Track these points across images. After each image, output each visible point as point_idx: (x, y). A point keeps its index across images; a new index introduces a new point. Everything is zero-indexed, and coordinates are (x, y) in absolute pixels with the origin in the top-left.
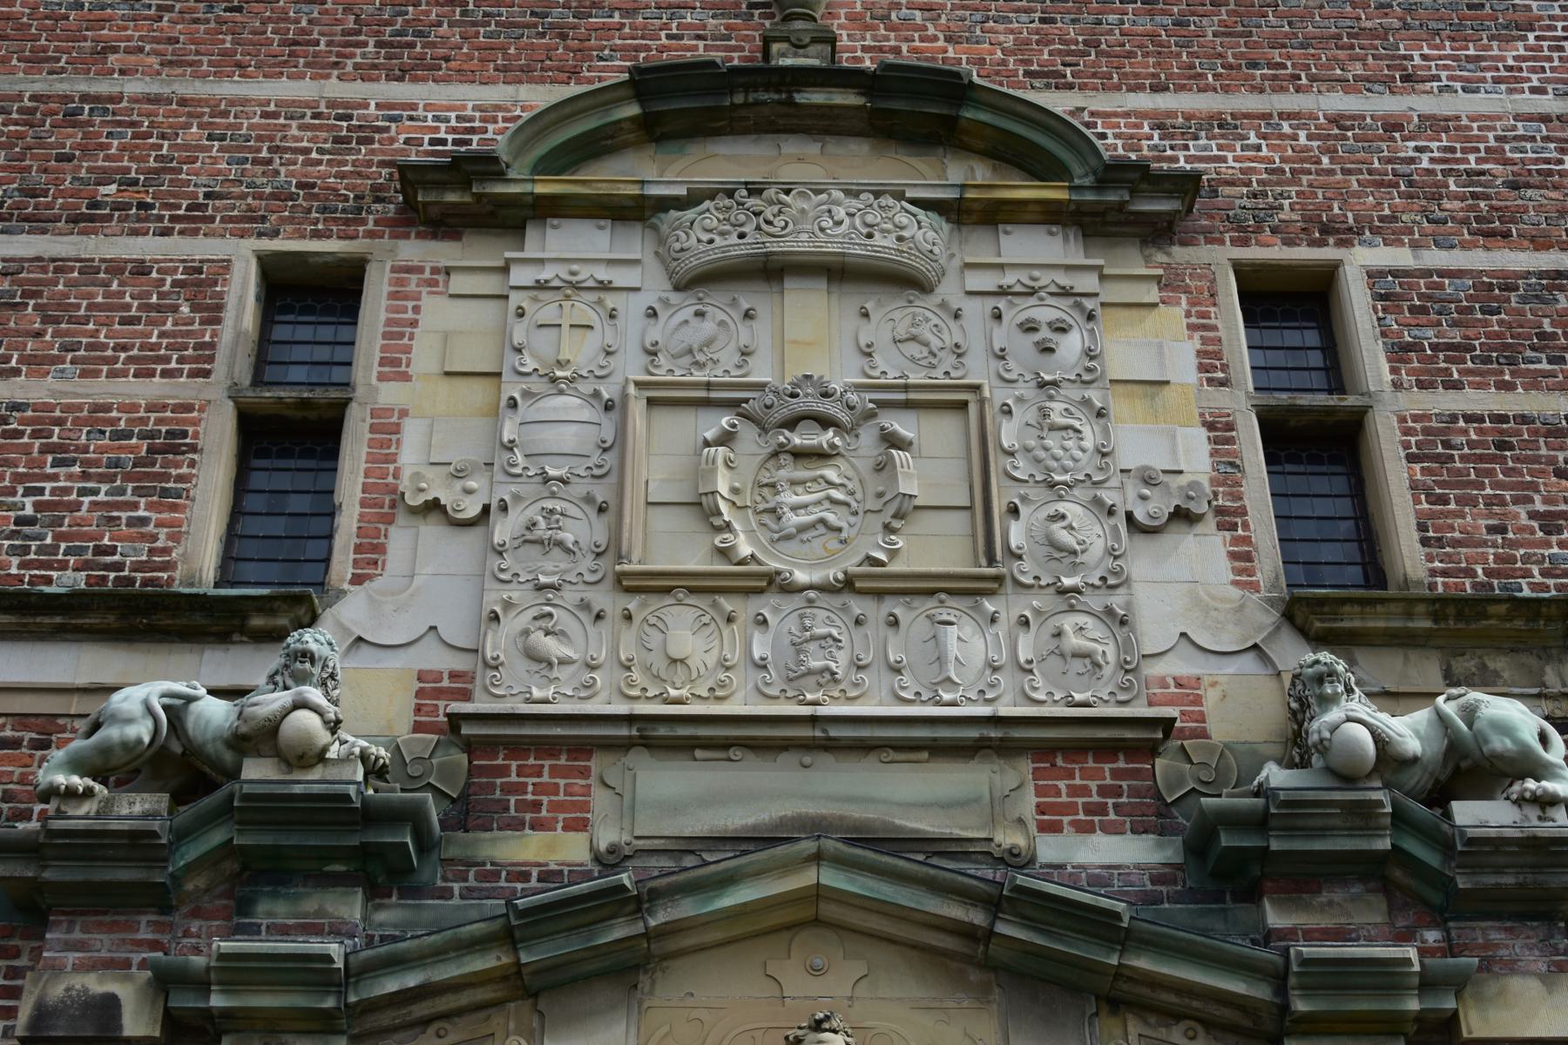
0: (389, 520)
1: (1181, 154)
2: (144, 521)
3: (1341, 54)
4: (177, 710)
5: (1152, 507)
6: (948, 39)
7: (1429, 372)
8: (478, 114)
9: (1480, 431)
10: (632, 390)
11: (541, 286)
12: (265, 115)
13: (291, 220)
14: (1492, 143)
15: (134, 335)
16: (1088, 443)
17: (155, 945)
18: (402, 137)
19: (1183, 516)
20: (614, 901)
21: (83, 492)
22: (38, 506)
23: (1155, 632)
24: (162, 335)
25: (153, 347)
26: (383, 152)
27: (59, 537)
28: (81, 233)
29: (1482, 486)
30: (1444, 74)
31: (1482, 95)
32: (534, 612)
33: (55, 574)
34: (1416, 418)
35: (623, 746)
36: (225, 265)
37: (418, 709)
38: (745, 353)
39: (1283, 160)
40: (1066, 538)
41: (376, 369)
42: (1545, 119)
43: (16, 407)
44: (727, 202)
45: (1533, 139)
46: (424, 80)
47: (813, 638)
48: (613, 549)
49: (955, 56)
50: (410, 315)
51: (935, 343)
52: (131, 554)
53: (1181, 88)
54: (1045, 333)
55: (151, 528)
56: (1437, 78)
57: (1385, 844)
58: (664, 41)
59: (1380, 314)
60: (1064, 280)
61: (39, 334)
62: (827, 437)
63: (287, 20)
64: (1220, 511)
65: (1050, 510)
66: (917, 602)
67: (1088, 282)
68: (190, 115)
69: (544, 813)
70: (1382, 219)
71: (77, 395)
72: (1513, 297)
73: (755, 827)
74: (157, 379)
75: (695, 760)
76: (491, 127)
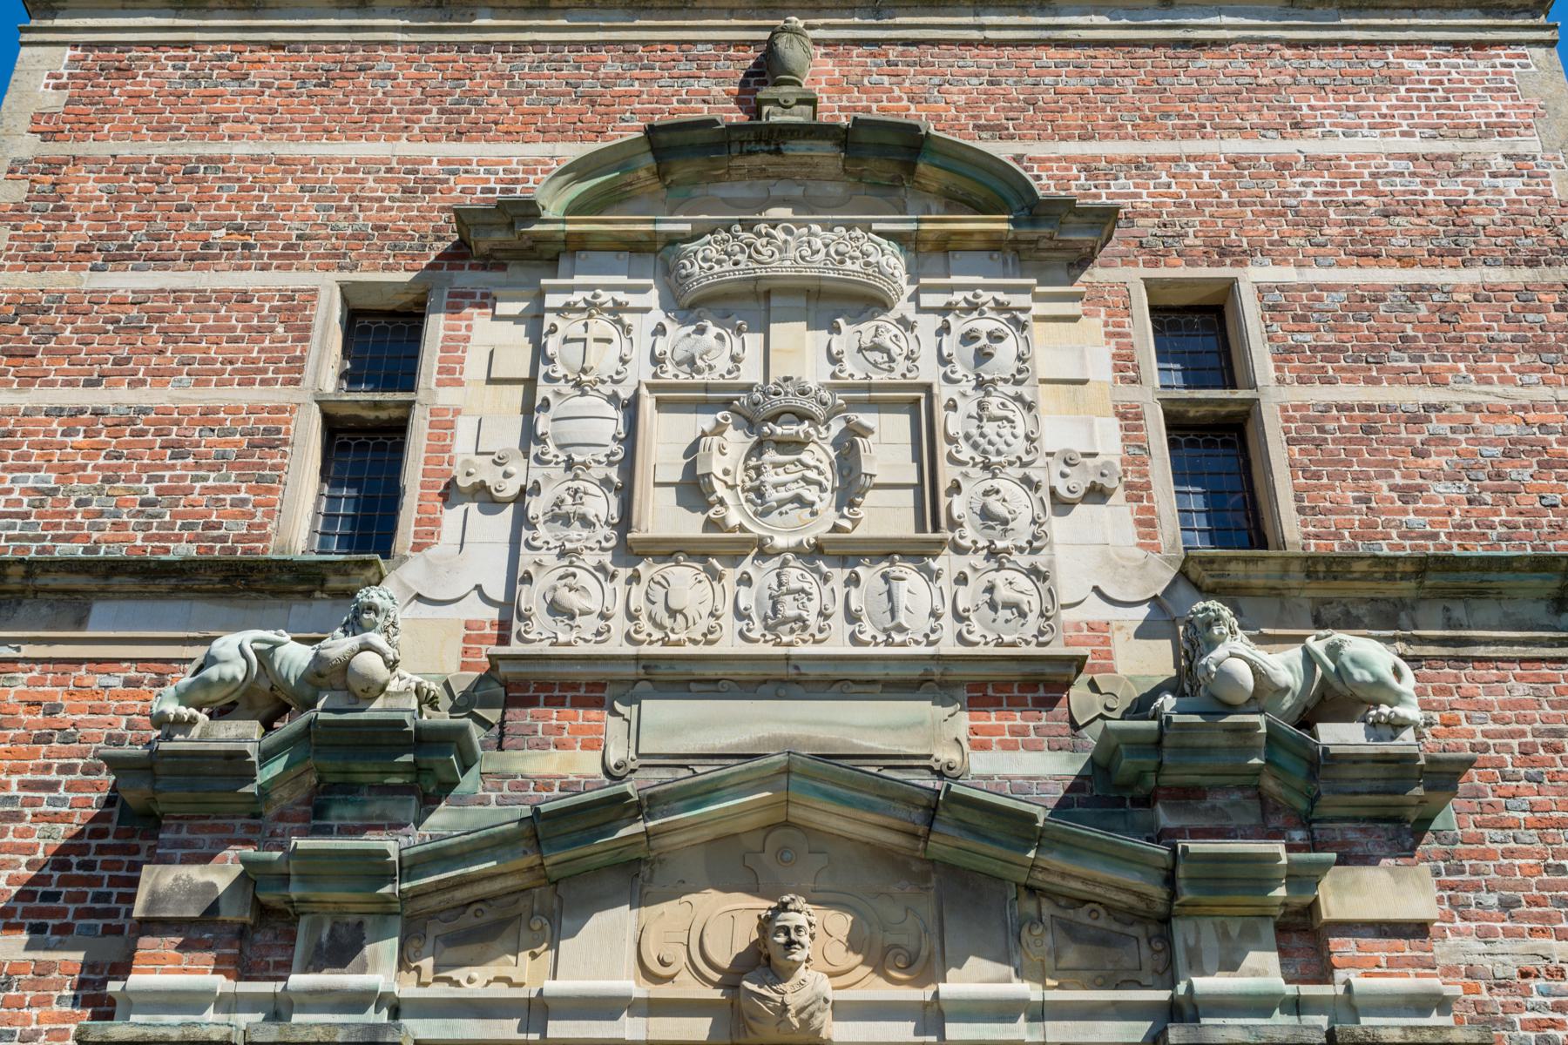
1: (1103, 192)
2: (244, 502)
3: (1241, 107)
5: (1071, 482)
6: (911, 100)
8: (521, 167)
9: (1351, 419)
10: (644, 391)
11: (568, 308)
12: (347, 171)
13: (367, 257)
14: (1367, 179)
15: (238, 351)
16: (1020, 431)
18: (459, 188)
19: (1097, 494)
20: (616, 808)
21: (195, 479)
22: (159, 491)
26: (444, 200)
27: (174, 516)
28: (196, 269)
29: (1350, 464)
30: (1327, 122)
31: (1359, 138)
32: (561, 571)
33: (172, 546)
34: (1296, 408)
36: (313, 293)
37: (465, 652)
38: (735, 359)
41: (435, 376)
42: (1413, 158)
43: (143, 411)
44: (725, 235)
45: (1402, 175)
46: (478, 140)
47: (789, 592)
48: (625, 522)
49: (915, 114)
50: (463, 332)
51: (895, 350)
52: (235, 528)
53: (1106, 136)
56: (1319, 125)
58: (676, 105)
59: (1268, 322)
61: (161, 352)
64: (1128, 486)
65: (987, 485)
68: (285, 172)
69: (565, 735)
70: (1272, 243)
71: (191, 400)
72: (1382, 307)
73: (737, 746)
74: (257, 387)
75: (690, 691)
76: (532, 178)
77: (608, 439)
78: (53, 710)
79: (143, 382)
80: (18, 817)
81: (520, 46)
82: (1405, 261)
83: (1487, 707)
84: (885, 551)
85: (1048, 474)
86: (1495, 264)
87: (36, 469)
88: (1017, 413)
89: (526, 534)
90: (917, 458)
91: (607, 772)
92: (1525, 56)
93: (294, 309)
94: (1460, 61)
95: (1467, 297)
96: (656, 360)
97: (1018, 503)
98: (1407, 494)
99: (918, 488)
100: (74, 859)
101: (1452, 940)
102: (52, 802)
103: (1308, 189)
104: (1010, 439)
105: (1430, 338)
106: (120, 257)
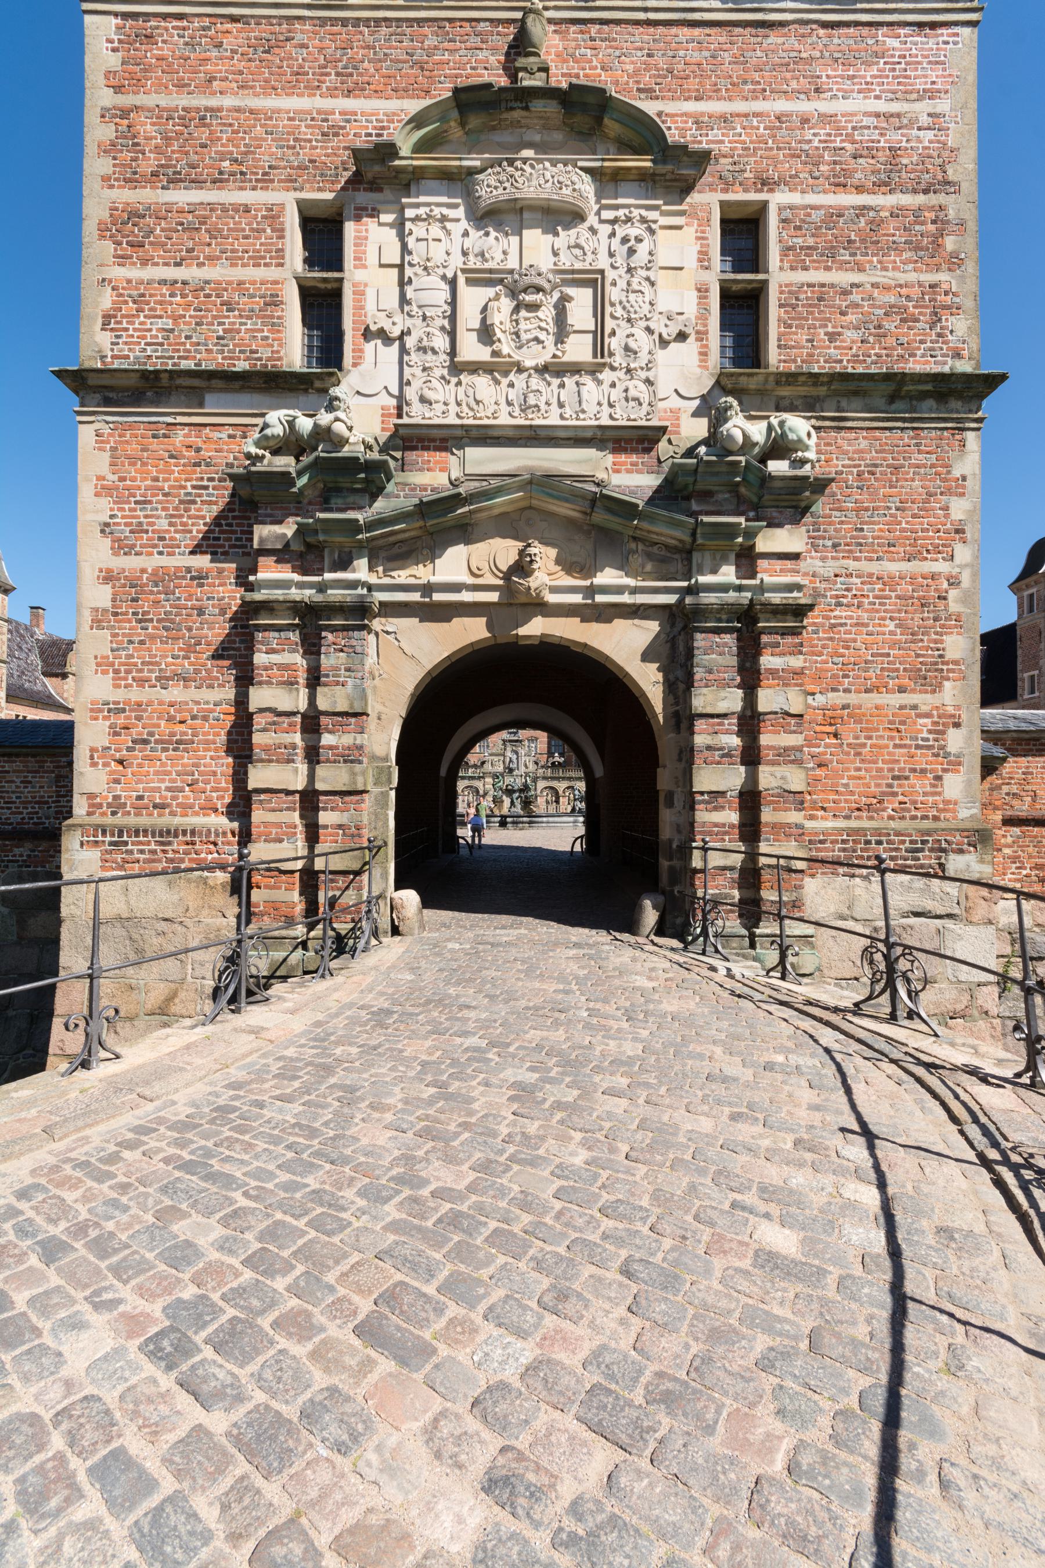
1: (704, 139)
2: (267, 338)
3: (788, 75)
5: (669, 330)
6: (602, 68)
9: (813, 292)
10: (459, 273)
11: (417, 219)
12: (290, 119)
13: (308, 181)
15: (249, 244)
16: (647, 300)
19: (682, 337)
20: (456, 500)
21: (241, 324)
22: (225, 331)
23: (664, 388)
24: (261, 244)
27: (235, 345)
28: (219, 189)
29: (807, 319)
30: (835, 87)
34: (787, 285)
38: (505, 253)
39: (751, 142)
40: (633, 345)
42: (877, 115)
43: (207, 282)
44: (498, 169)
48: (453, 352)
49: (603, 80)
51: (587, 248)
52: (265, 353)
53: (710, 98)
56: (831, 90)
61: (209, 245)
63: (291, 58)
64: (698, 332)
65: (628, 332)
72: (841, 220)
77: (442, 303)
78: (198, 450)
79: (203, 264)
80: (194, 502)
82: (859, 189)
83: (846, 453)
84: (575, 369)
85: (658, 325)
87: (161, 317)
88: (646, 287)
89: (406, 358)
90: (595, 315)
91: (451, 483)
92: (957, 35)
93: (273, 214)
94: (919, 39)
95: (887, 214)
96: (465, 254)
97: (643, 342)
98: (832, 337)
99: (595, 333)
101: (809, 560)
102: (208, 495)
103: (815, 137)
105: (863, 241)
106: (175, 181)
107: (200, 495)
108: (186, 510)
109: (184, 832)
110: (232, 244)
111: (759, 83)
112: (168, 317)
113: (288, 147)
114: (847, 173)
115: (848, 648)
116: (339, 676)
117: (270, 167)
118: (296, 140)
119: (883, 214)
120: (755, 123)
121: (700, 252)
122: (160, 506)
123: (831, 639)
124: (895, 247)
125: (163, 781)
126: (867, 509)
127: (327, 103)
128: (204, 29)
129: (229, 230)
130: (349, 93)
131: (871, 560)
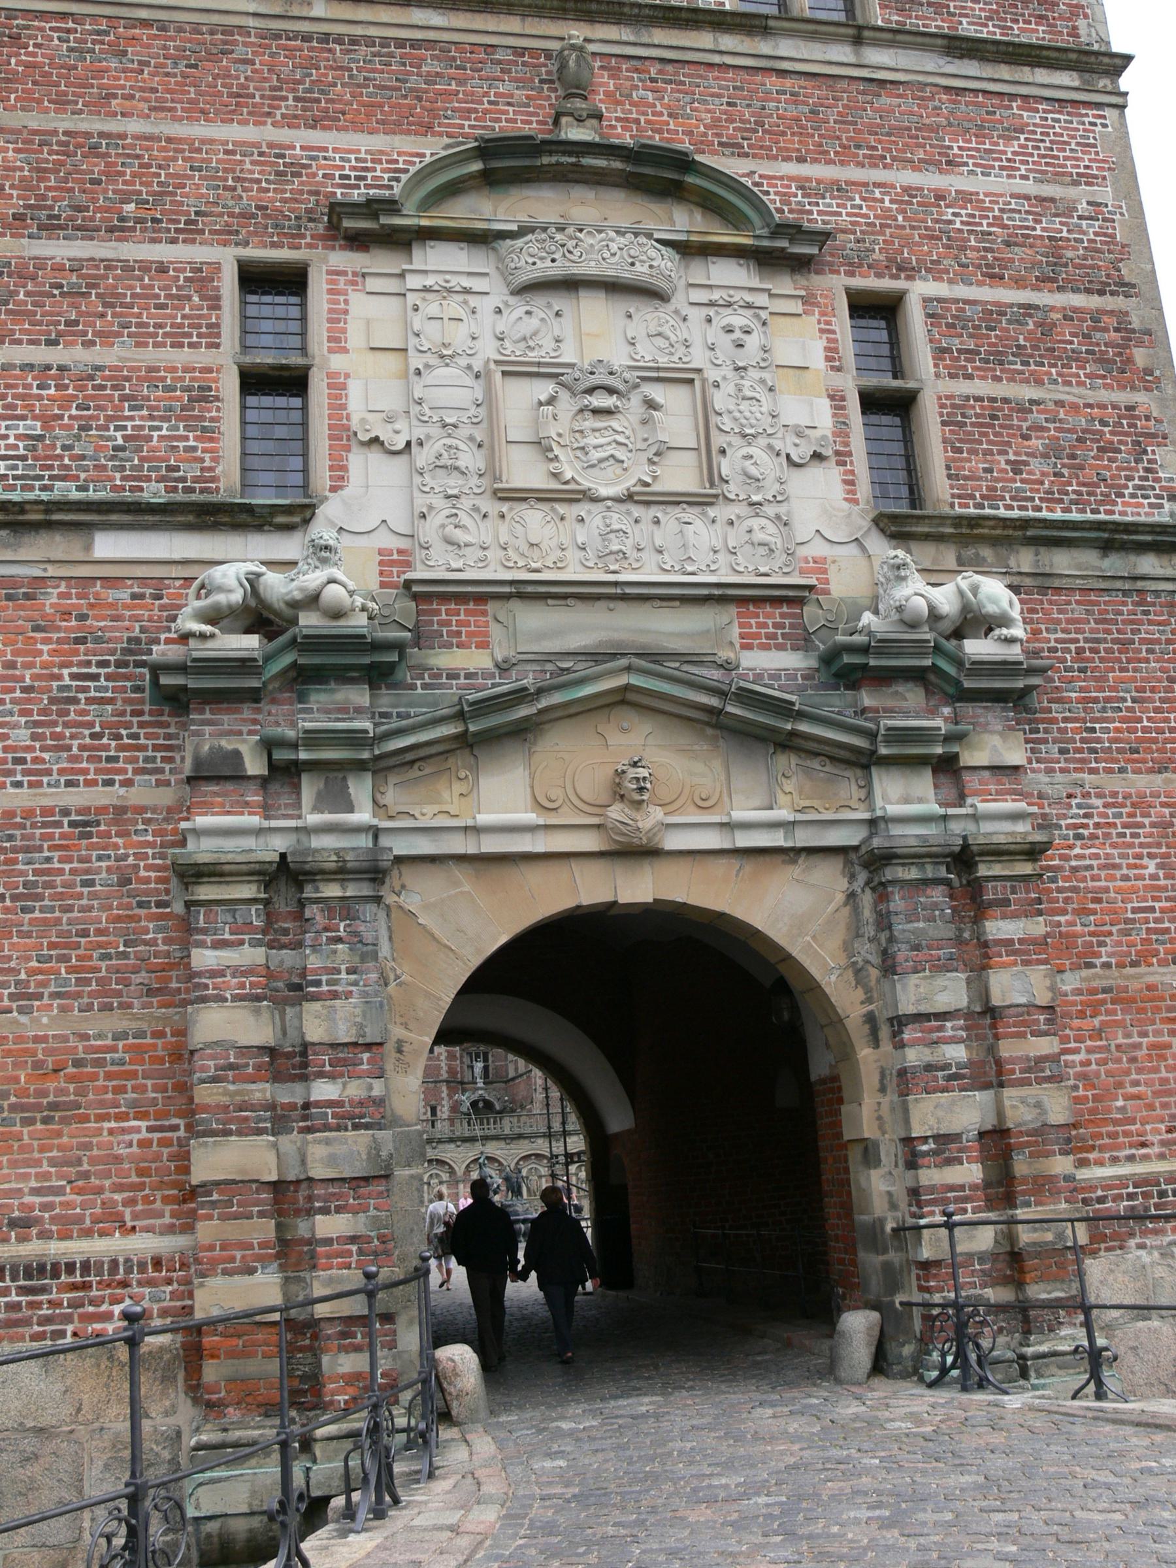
0: (348, 449)
1: (815, 209)
2: (194, 449)
4: (253, 580)
5: (800, 450)
6: (670, 115)
7: (955, 367)
9: (982, 407)
10: (492, 366)
11: (426, 290)
12: (227, 152)
13: (256, 233)
14: (997, 213)
17: (255, 722)
18: (321, 173)
19: (817, 456)
21: (152, 428)
23: (803, 530)
24: (184, 317)
25: (181, 326)
26: (309, 184)
27: (142, 459)
28: (119, 239)
30: (971, 161)
31: (992, 178)
32: (447, 512)
33: (144, 485)
34: (948, 397)
35: (507, 597)
36: (217, 267)
37: (381, 573)
39: (876, 217)
40: (753, 471)
41: (326, 345)
42: (1027, 198)
43: (98, 368)
44: (544, 236)
45: (1019, 212)
46: (329, 128)
48: (492, 471)
50: (342, 306)
51: (673, 338)
52: (190, 471)
53: (815, 161)
54: (738, 334)
55: (199, 453)
56: (966, 164)
57: (928, 662)
58: (486, 106)
60: (749, 298)
62: (608, 401)
63: (229, 76)
64: (837, 453)
66: (669, 509)
67: (761, 300)
68: (176, 150)
70: (932, 262)
76: (378, 167)
79: (93, 343)
80: (75, 701)
81: (354, 41)
82: (1019, 283)
83: (1058, 621)
85: (787, 444)
86: (1075, 290)
87: (23, 418)
91: (497, 666)
92: (1104, 117)
94: (1062, 117)
95: (1059, 316)
98: (1017, 467)
100: (124, 732)
101: (1030, 775)
102: (97, 689)
103: (957, 218)
104: (759, 416)
105: (1035, 348)
106: (51, 227)
107: (85, 690)
108: (64, 713)
109: (70, 1268)
110: (139, 315)
111: (875, 148)
112: (35, 418)
113: (225, 188)
114: (1005, 264)
115: (1098, 901)
116: (336, 982)
117: (197, 213)
118: (235, 179)
119: (1056, 316)
120: (878, 195)
121: (827, 349)
122: (16, 708)
123: (1075, 889)
124: (1075, 357)
125: (25, 1177)
126: (1096, 700)
127: (284, 135)
128: (98, 33)
129: (133, 296)
130: (314, 124)
131: (1109, 771)
